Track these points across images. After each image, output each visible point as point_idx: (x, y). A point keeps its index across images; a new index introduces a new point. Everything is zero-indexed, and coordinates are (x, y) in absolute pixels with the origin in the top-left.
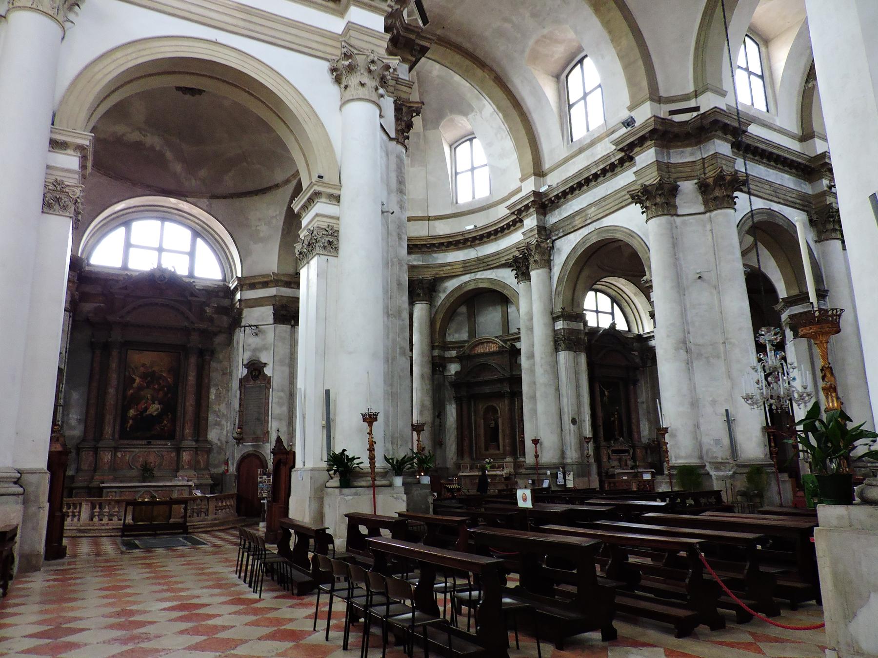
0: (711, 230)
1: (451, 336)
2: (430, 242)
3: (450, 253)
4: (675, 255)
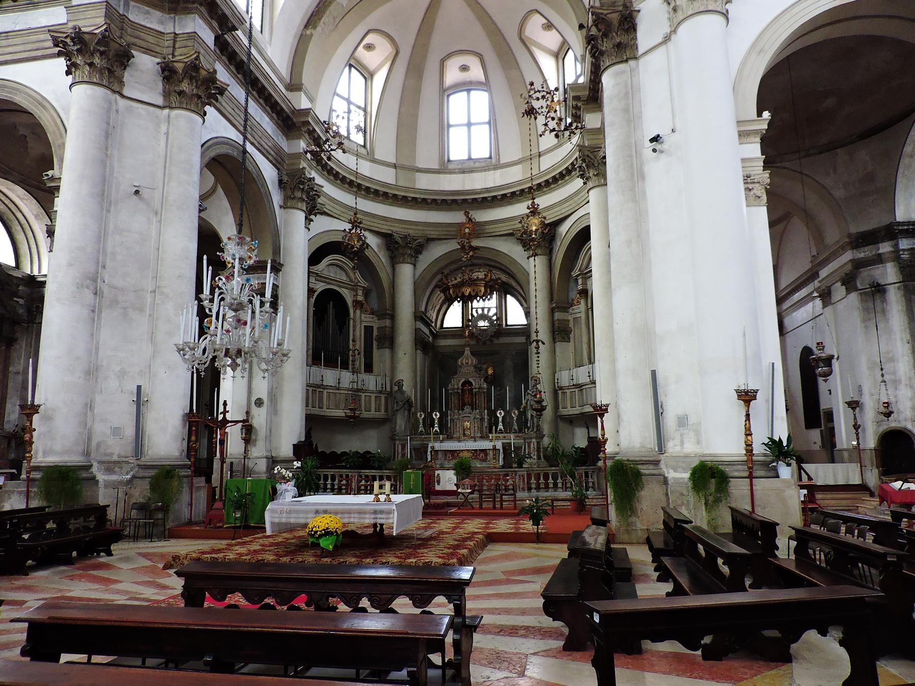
0: (167, 134)
4: (107, 148)
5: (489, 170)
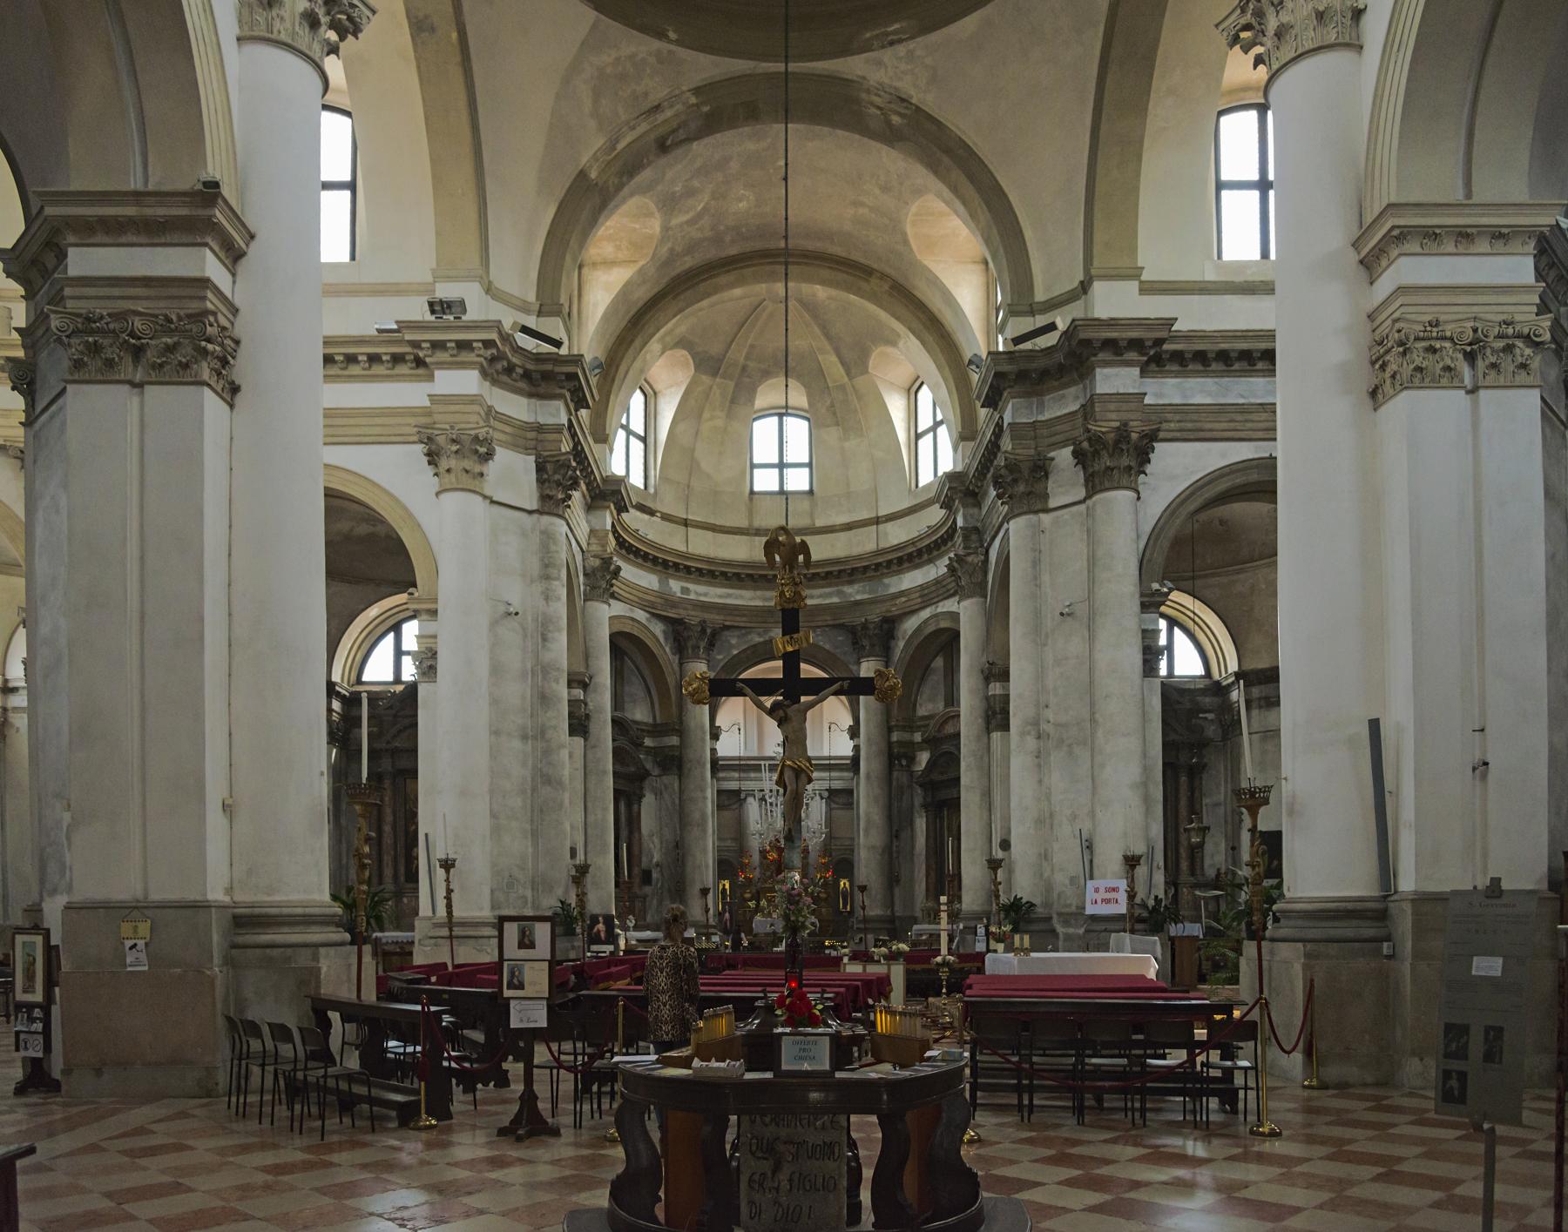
1: (924, 709)
2: (875, 562)
3: (906, 575)
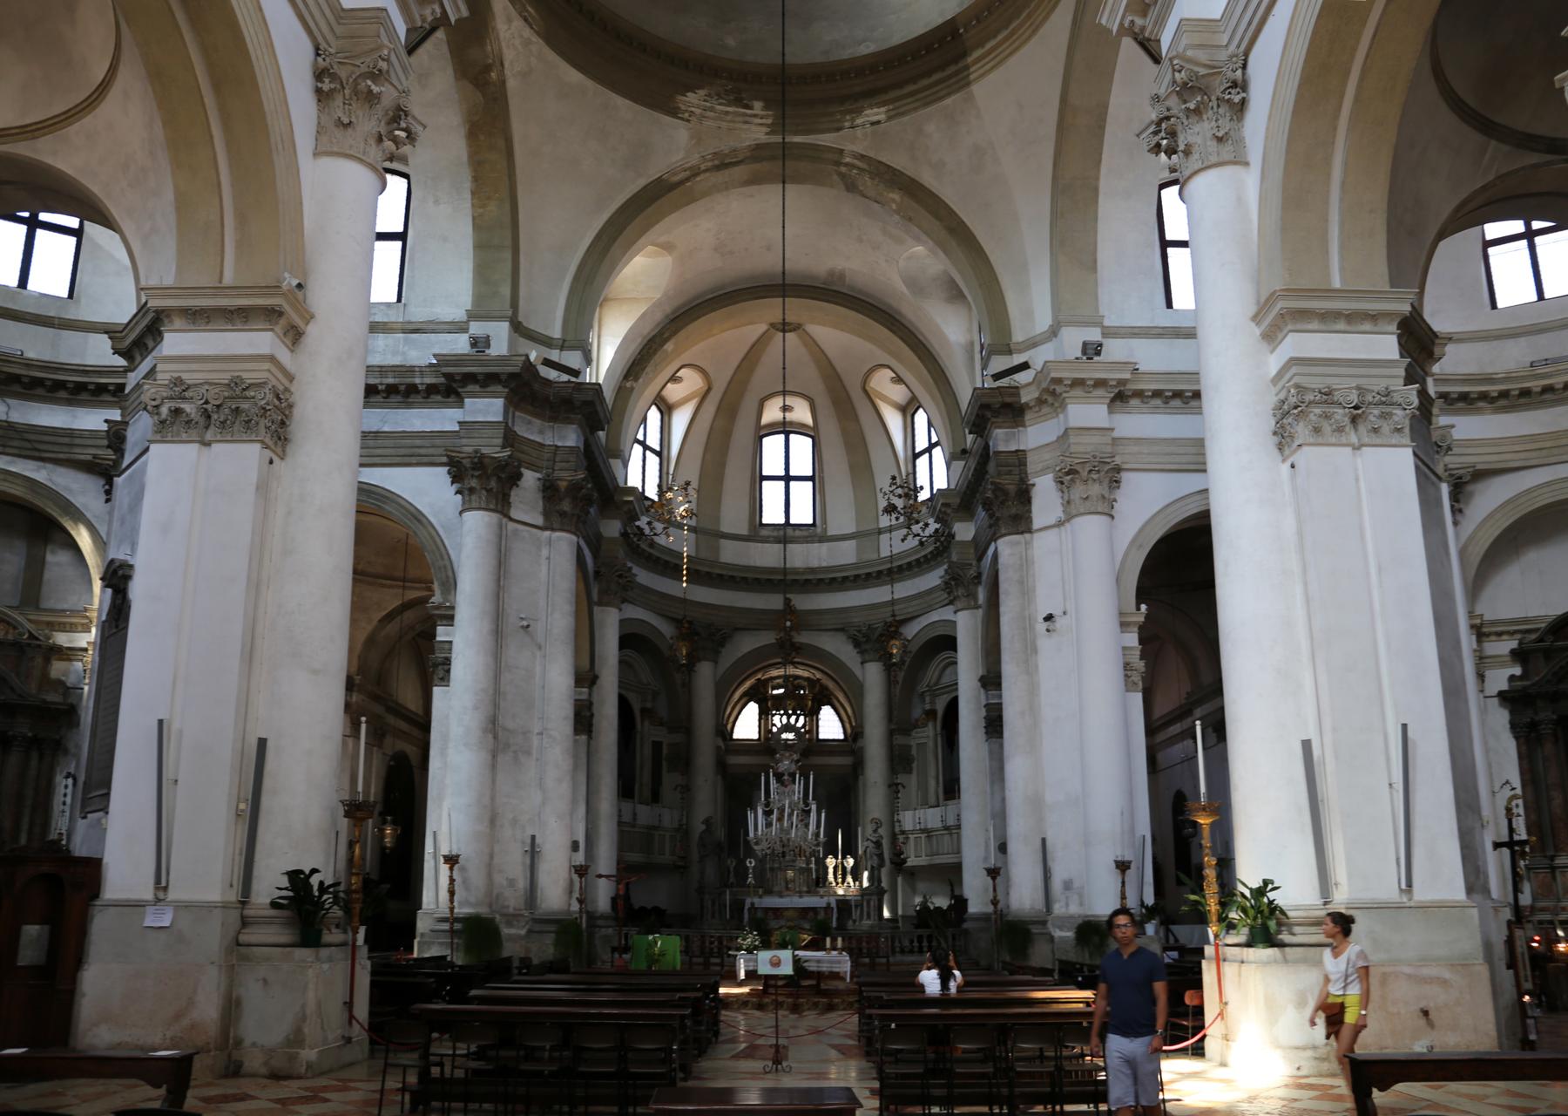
5: (812, 542)
